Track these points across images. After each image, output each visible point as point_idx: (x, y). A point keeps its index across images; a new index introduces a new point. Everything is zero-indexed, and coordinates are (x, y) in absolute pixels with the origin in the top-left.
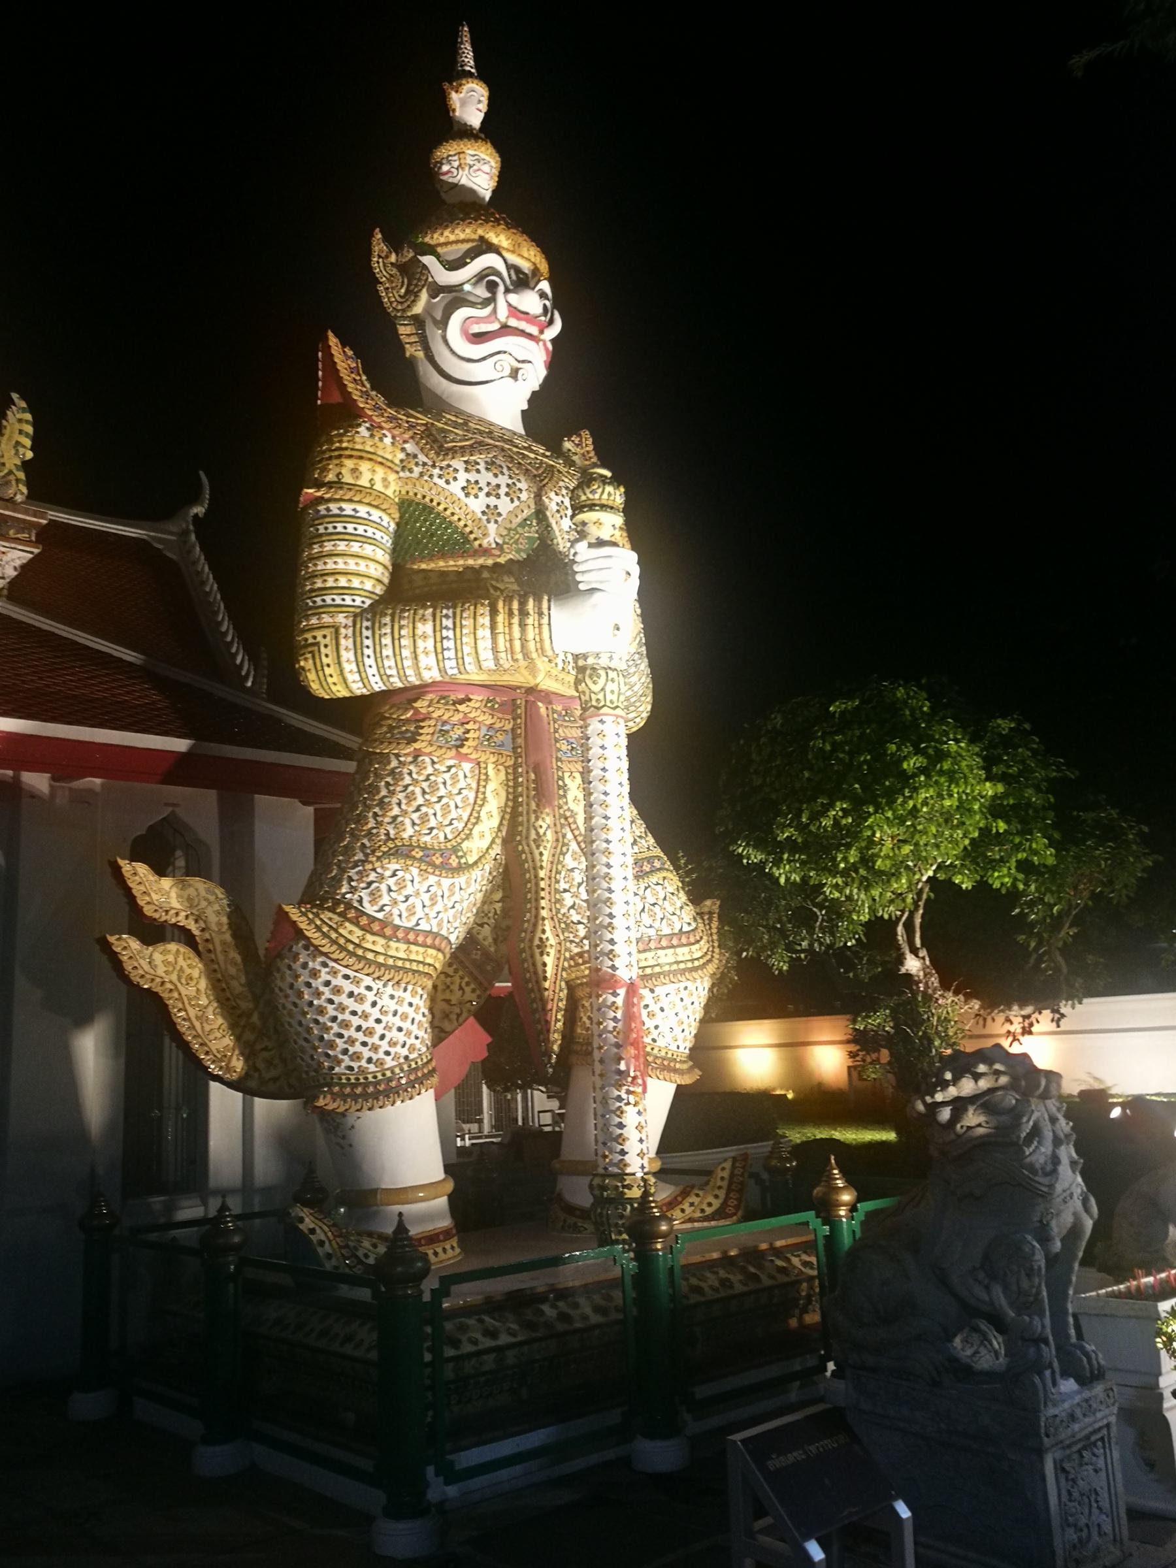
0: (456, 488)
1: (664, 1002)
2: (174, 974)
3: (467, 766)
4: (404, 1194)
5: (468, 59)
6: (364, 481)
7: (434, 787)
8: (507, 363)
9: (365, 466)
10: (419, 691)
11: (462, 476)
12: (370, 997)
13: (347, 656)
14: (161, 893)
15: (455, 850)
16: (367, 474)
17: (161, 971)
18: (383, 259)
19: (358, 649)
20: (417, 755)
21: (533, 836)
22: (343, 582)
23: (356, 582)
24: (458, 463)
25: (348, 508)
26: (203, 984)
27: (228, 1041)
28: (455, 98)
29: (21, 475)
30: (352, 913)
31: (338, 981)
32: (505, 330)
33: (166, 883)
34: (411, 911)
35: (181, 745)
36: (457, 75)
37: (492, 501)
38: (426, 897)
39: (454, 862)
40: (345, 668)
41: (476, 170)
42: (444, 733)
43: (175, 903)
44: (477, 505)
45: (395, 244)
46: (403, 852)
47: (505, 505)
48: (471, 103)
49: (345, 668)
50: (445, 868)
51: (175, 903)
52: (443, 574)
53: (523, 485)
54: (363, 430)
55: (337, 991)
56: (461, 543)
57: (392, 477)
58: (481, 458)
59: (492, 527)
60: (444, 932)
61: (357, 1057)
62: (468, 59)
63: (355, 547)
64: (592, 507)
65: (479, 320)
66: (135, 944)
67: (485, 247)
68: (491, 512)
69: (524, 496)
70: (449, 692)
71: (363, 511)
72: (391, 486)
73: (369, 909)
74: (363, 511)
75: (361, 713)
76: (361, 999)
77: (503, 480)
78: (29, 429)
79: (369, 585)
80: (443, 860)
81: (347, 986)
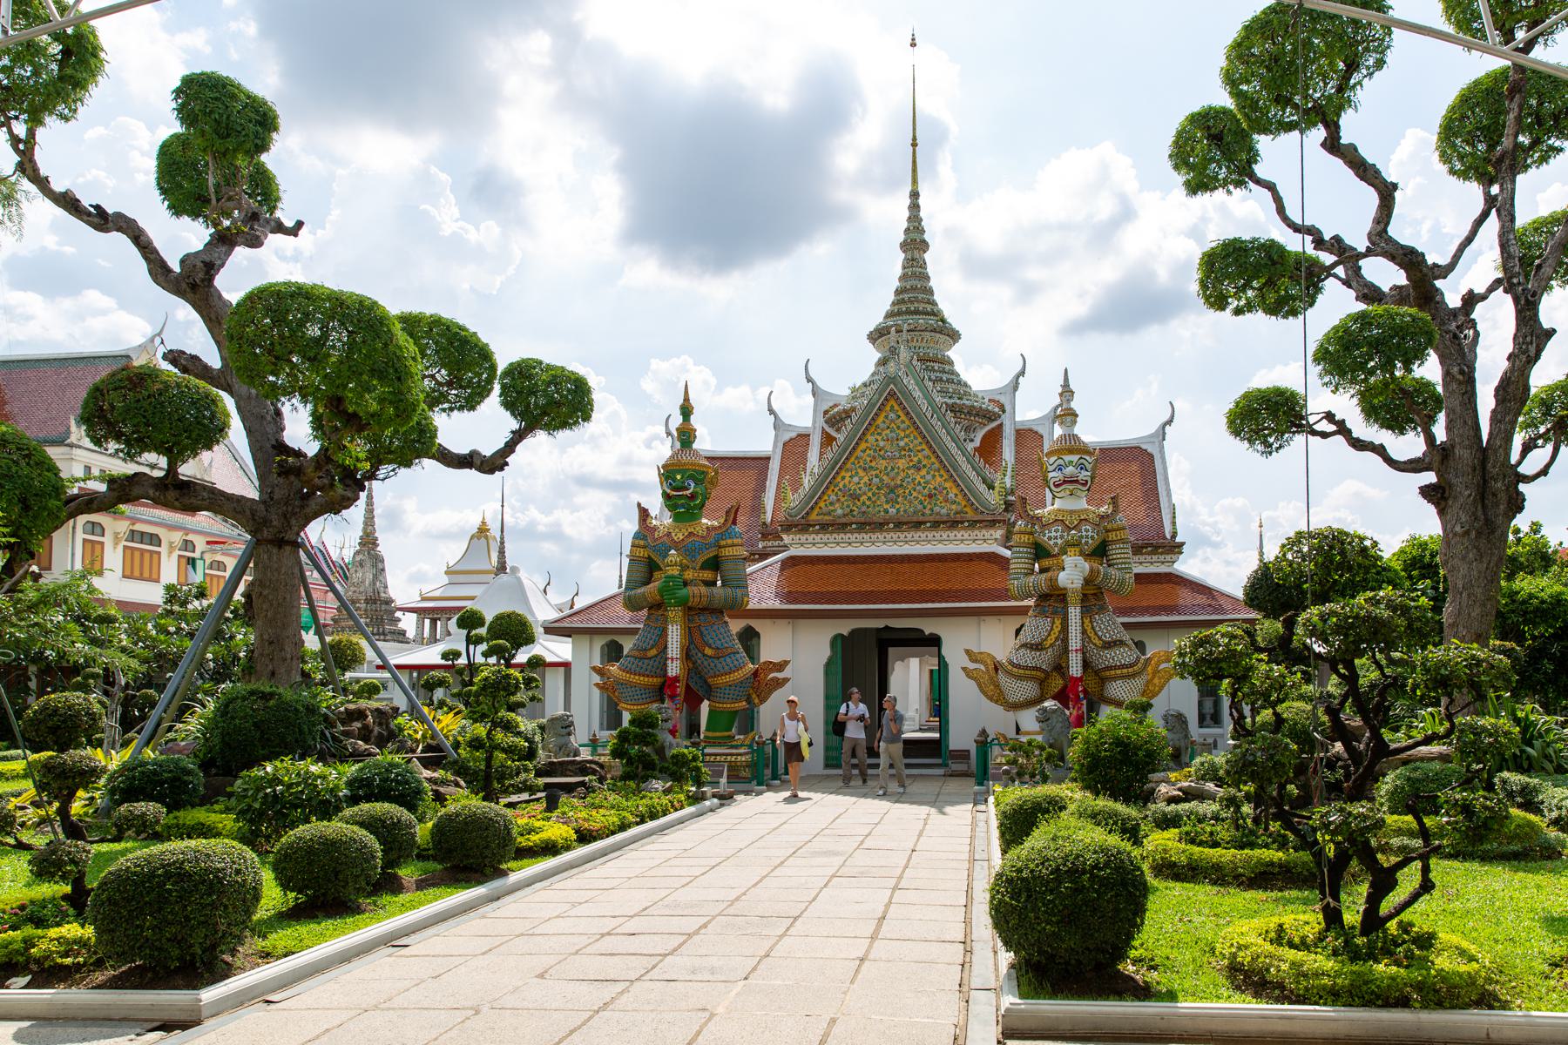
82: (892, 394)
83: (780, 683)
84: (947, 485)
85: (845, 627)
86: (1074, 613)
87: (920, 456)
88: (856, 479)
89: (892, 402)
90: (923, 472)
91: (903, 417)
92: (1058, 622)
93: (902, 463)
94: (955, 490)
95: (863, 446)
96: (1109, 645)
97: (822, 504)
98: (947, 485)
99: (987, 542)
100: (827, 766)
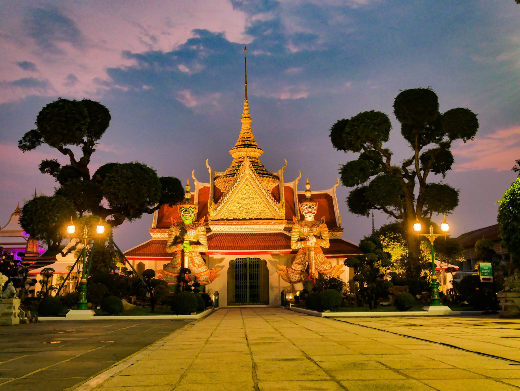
67: (306, 205)
82: (247, 179)
83: (216, 276)
84: (266, 209)
85: (234, 257)
86: (313, 253)
87: (257, 200)
88: (235, 208)
89: (247, 181)
90: (258, 205)
91: (251, 186)
92: (307, 256)
93: (251, 202)
94: (268, 211)
95: (237, 196)
96: (322, 263)
99: (280, 228)
100: (228, 305)
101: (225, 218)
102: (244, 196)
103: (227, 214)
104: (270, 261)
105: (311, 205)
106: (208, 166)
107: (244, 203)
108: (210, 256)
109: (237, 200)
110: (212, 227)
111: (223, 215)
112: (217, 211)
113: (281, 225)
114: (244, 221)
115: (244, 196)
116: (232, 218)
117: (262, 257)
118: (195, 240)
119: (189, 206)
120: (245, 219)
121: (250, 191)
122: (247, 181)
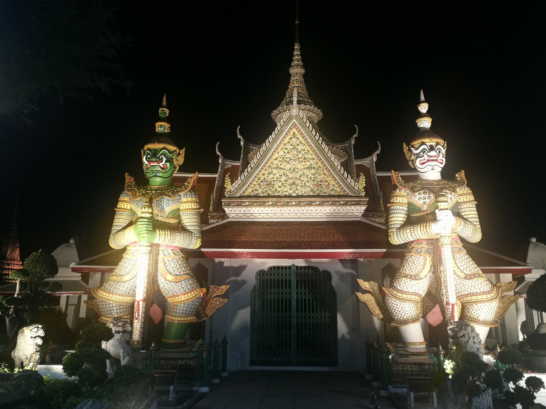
0: (417, 199)
1: (480, 308)
2: (368, 299)
3: (422, 257)
4: (415, 344)
5: (422, 98)
6: (398, 201)
7: (414, 262)
8: (431, 167)
9: (398, 198)
10: (412, 242)
11: (418, 196)
12: (399, 305)
13: (396, 237)
14: (365, 285)
15: (418, 275)
16: (399, 200)
17: (366, 299)
18: (405, 148)
19: (397, 236)
20: (411, 255)
21: (439, 271)
22: (395, 223)
23: (397, 222)
24: (417, 194)
25: (395, 207)
26: (374, 301)
27: (379, 312)
28: (419, 108)
29: (363, 190)
30: (395, 289)
31: (392, 301)
32: (428, 161)
33: (366, 283)
34: (407, 288)
35: (384, 250)
36: (419, 102)
37: (425, 200)
38: (411, 285)
39: (417, 278)
40: (396, 239)
41: (425, 123)
42: (417, 250)
43: (368, 286)
44: (421, 202)
45: (408, 145)
46: (406, 276)
47: (427, 201)
48: (424, 108)
49: (396, 239)
50: (415, 279)
51: (368, 286)
52: (416, 217)
53: (432, 195)
54: (398, 191)
55: (393, 303)
56: (419, 210)
57: (405, 199)
58: (422, 192)
59: (425, 206)
60: (417, 292)
61: (398, 316)
62: (422, 98)
63: (397, 215)
64: (438, 202)
65: (422, 160)
66: (360, 294)
67: (423, 143)
68: (425, 203)
69: (432, 198)
70: (418, 241)
71: (398, 207)
72: (405, 200)
73: (399, 288)
74: (398, 207)
75: (405, 246)
76: (397, 305)
77: (427, 196)
78: (364, 180)
79: (400, 222)
80: (415, 277)
81: (394, 303)
88: (271, 176)
89: (294, 130)
91: (301, 139)
93: (300, 166)
94: (333, 183)
97: (250, 190)
98: (328, 179)
100: (252, 363)
101: (252, 194)
102: (288, 155)
103: (257, 187)
104: (337, 272)
105: (434, 144)
106: (239, 137)
107: (288, 167)
108: (217, 260)
109: (276, 162)
110: (227, 210)
111: (250, 190)
112: (239, 181)
113: (358, 207)
114: (288, 200)
115: (288, 155)
116: (266, 194)
117: (322, 263)
118: (173, 221)
119: (162, 146)
120: (290, 196)
121: (300, 148)
122: (294, 130)
